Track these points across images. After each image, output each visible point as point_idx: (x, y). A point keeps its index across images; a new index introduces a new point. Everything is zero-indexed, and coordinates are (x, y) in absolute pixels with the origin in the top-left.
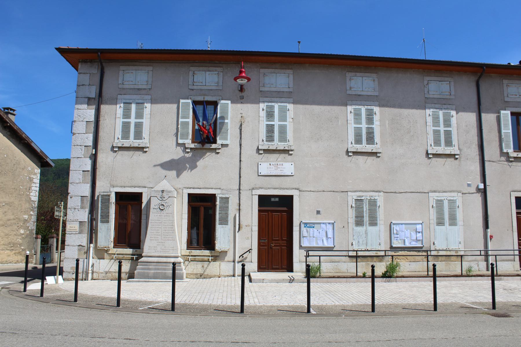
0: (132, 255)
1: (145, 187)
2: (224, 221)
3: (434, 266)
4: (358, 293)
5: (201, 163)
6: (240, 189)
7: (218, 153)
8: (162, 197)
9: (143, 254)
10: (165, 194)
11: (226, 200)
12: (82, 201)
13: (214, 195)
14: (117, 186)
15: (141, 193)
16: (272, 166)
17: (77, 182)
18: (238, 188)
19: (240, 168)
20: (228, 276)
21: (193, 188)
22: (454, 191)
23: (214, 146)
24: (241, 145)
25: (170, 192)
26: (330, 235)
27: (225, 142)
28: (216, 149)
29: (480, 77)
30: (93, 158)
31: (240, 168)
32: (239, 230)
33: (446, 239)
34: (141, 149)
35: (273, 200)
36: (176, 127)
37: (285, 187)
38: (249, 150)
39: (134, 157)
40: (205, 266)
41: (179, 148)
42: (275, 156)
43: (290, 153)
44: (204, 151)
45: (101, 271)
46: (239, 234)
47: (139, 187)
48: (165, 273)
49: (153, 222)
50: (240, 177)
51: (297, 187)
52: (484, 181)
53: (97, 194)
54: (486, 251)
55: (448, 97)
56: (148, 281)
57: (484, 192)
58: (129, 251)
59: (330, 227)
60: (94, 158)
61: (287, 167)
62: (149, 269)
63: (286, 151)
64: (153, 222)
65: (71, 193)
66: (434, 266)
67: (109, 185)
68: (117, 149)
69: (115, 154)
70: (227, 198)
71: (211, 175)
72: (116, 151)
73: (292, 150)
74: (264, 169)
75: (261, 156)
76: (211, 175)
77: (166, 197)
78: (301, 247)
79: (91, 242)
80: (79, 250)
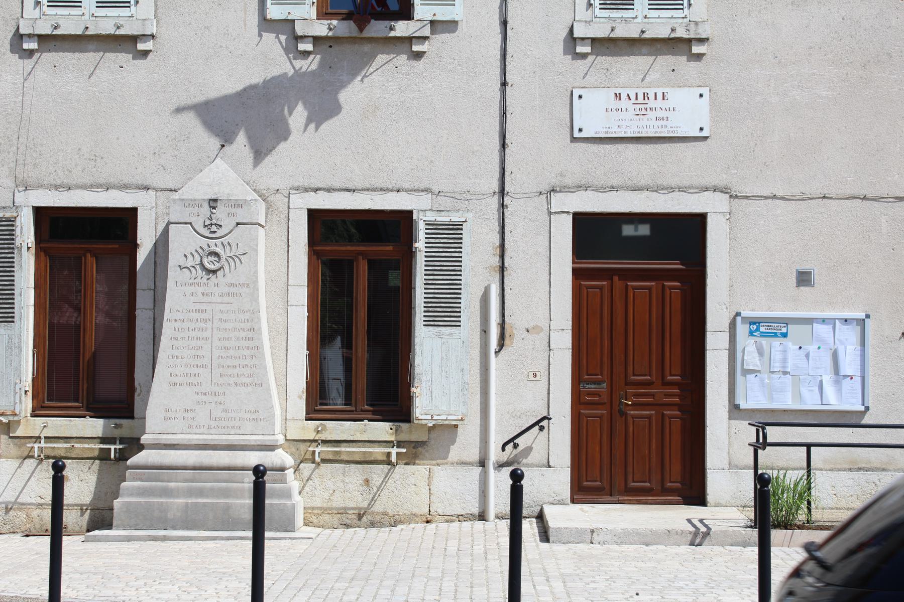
0: (103, 440)
2: (446, 313)
5: (352, 95)
6: (502, 193)
7: (419, 55)
8: (212, 225)
9: (145, 439)
10: (220, 214)
11: (450, 234)
13: (407, 216)
14: (40, 186)
15: (133, 211)
16: (624, 103)
18: (495, 186)
19: (504, 113)
20: (462, 518)
21: (329, 190)
23: (402, 28)
24: (504, 23)
25: (238, 205)
26: (850, 364)
27: (443, 13)
28: (410, 40)
31: (504, 113)
32: (501, 345)
34: (126, 43)
35: (628, 230)
37: (674, 182)
39: (103, 74)
40: (377, 480)
41: (269, 37)
42: (637, 63)
43: (696, 49)
44: (367, 48)
46: (501, 360)
47: (124, 187)
48: (228, 507)
49: (179, 316)
50: (504, 146)
51: (721, 181)
56: (165, 539)
58: (94, 426)
59: (850, 335)
61: (684, 105)
62: (166, 492)
64: (179, 316)
67: (10, 183)
68: (33, 45)
69: (29, 63)
70: (457, 227)
71: (389, 139)
72: (31, 53)
73: (702, 41)
74: (596, 113)
75: (582, 65)
76: (389, 139)
77: (227, 224)
78: (735, 410)
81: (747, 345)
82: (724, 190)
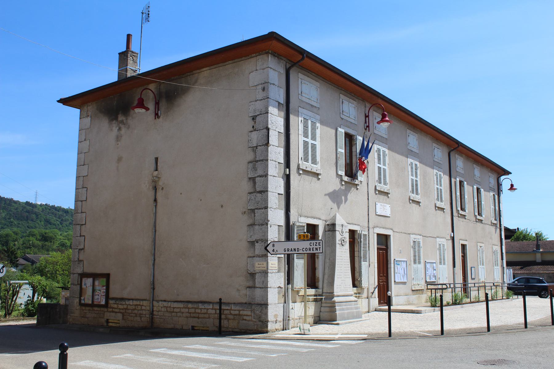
0: (315, 295)
1: (320, 219)
3: (441, 296)
4: (429, 321)
9: (335, 294)
12: (279, 231)
17: (275, 207)
20: (366, 312)
22: (443, 238)
29: (452, 150)
30: (285, 179)
33: (445, 274)
34: (316, 175)
36: (335, 157)
38: (372, 191)
44: (351, 185)
45: (296, 317)
52: (453, 231)
53: (291, 223)
54: (454, 284)
55: (440, 162)
57: (453, 239)
60: (287, 179)
62: (351, 309)
63: (387, 194)
65: (271, 221)
66: (441, 296)
67: (297, 214)
79: (288, 284)
80: (279, 293)
81: (396, 265)
82: (392, 229)
